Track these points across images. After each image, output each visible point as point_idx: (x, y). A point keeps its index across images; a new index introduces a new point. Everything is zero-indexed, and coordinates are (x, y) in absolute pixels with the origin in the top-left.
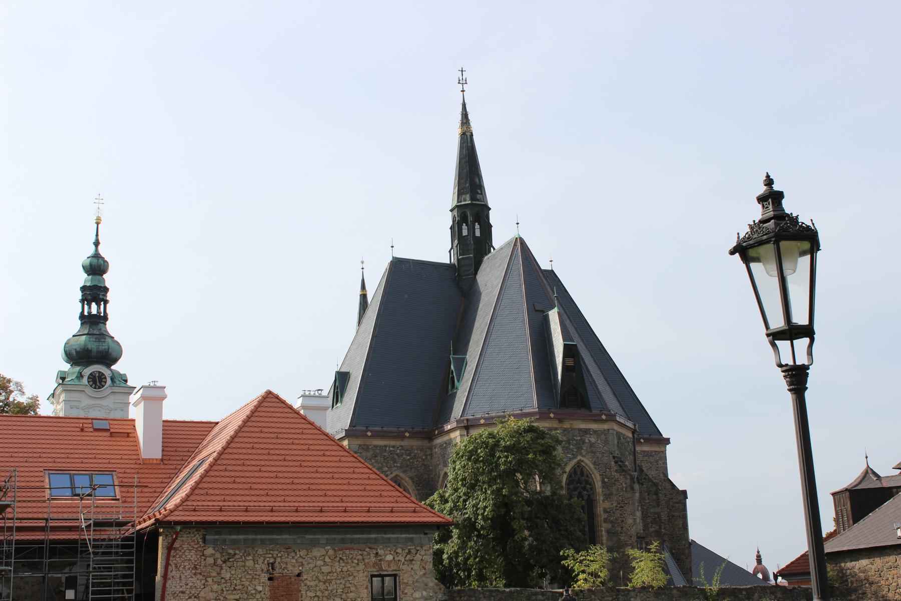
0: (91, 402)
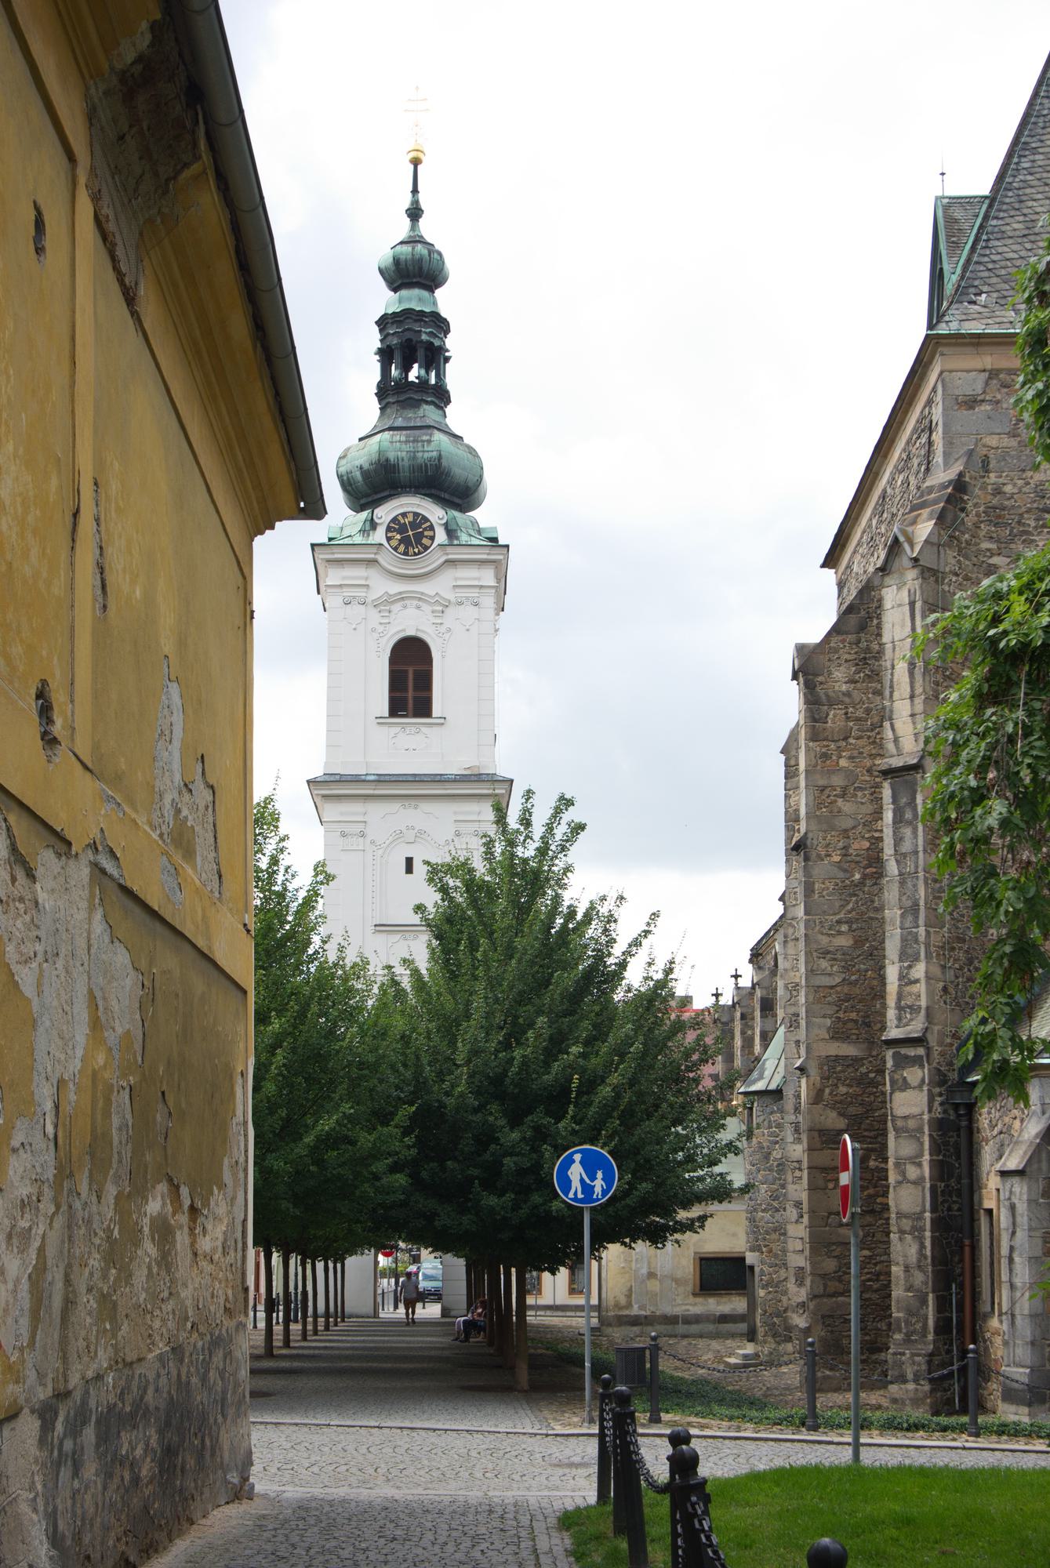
0: (396, 588)
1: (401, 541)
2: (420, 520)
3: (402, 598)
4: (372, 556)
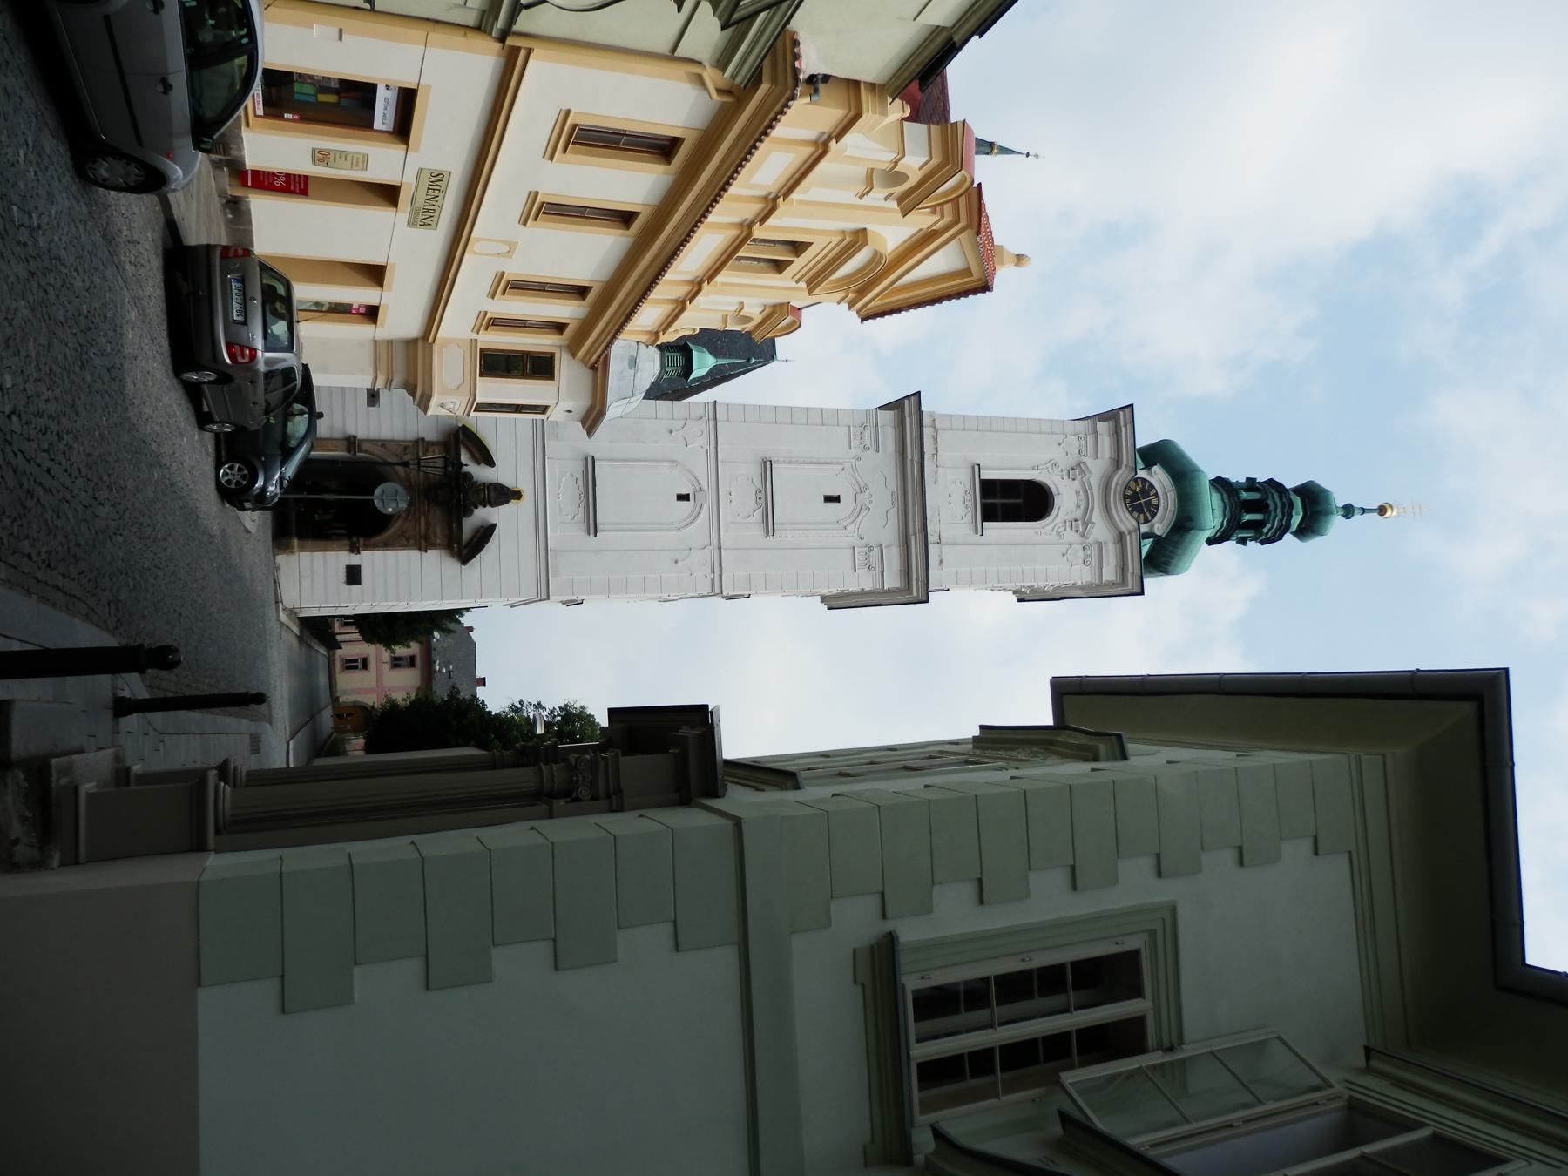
1: (1134, 491)
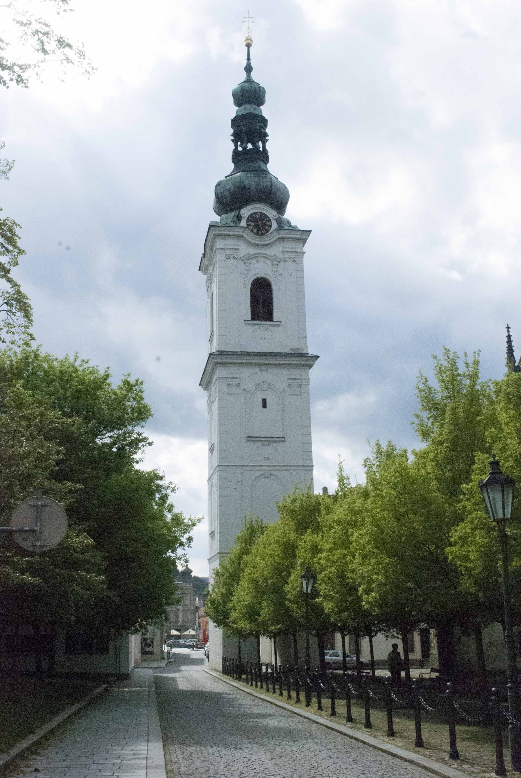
0: (252, 251)
1: (255, 227)
2: (263, 217)
3: (256, 256)
4: (241, 233)
